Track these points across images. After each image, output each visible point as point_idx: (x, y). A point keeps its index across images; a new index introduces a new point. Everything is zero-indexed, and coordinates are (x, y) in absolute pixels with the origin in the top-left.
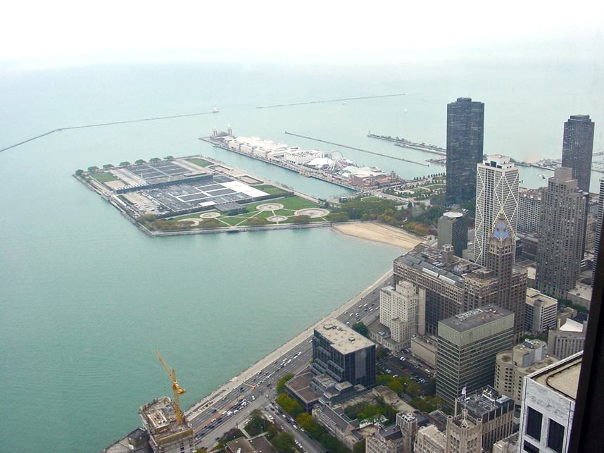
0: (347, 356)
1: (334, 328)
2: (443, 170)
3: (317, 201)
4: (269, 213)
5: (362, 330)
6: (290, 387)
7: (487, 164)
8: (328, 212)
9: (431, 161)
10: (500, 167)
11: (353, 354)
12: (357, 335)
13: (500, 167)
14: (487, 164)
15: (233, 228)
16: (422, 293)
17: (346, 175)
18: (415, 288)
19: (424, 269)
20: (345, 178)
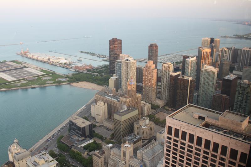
0: (83, 128)
1: (77, 119)
2: (108, 63)
3: (64, 75)
4: (46, 80)
5: (86, 118)
6: (62, 141)
7: (125, 60)
8: (68, 79)
9: (103, 60)
10: (130, 61)
11: (85, 127)
12: (85, 121)
13: (130, 61)
14: (125, 60)
15: (33, 86)
16: (106, 104)
17: (73, 66)
18: (103, 103)
19: (106, 97)
20: (73, 67)
